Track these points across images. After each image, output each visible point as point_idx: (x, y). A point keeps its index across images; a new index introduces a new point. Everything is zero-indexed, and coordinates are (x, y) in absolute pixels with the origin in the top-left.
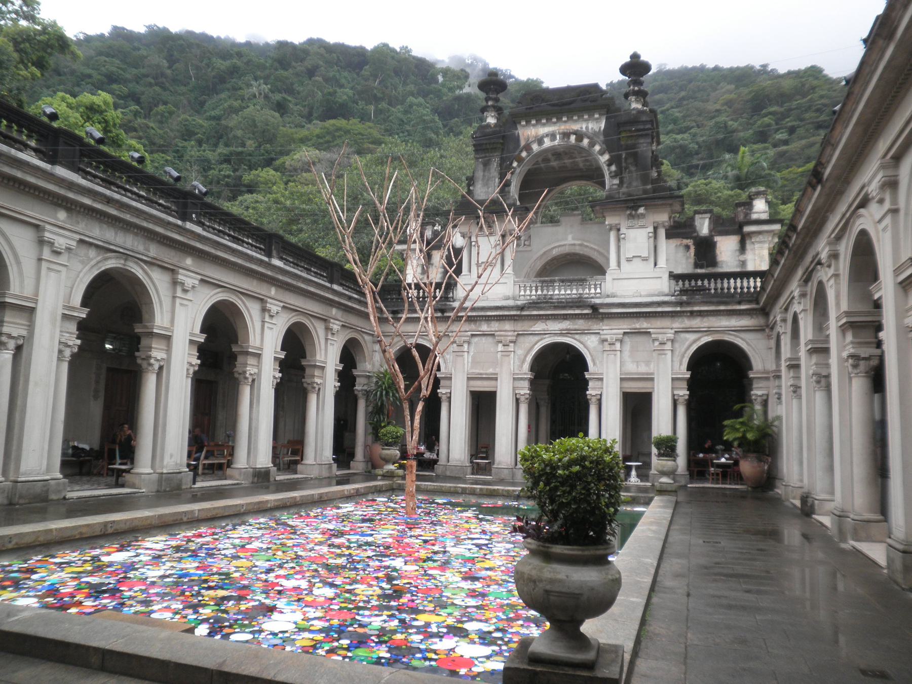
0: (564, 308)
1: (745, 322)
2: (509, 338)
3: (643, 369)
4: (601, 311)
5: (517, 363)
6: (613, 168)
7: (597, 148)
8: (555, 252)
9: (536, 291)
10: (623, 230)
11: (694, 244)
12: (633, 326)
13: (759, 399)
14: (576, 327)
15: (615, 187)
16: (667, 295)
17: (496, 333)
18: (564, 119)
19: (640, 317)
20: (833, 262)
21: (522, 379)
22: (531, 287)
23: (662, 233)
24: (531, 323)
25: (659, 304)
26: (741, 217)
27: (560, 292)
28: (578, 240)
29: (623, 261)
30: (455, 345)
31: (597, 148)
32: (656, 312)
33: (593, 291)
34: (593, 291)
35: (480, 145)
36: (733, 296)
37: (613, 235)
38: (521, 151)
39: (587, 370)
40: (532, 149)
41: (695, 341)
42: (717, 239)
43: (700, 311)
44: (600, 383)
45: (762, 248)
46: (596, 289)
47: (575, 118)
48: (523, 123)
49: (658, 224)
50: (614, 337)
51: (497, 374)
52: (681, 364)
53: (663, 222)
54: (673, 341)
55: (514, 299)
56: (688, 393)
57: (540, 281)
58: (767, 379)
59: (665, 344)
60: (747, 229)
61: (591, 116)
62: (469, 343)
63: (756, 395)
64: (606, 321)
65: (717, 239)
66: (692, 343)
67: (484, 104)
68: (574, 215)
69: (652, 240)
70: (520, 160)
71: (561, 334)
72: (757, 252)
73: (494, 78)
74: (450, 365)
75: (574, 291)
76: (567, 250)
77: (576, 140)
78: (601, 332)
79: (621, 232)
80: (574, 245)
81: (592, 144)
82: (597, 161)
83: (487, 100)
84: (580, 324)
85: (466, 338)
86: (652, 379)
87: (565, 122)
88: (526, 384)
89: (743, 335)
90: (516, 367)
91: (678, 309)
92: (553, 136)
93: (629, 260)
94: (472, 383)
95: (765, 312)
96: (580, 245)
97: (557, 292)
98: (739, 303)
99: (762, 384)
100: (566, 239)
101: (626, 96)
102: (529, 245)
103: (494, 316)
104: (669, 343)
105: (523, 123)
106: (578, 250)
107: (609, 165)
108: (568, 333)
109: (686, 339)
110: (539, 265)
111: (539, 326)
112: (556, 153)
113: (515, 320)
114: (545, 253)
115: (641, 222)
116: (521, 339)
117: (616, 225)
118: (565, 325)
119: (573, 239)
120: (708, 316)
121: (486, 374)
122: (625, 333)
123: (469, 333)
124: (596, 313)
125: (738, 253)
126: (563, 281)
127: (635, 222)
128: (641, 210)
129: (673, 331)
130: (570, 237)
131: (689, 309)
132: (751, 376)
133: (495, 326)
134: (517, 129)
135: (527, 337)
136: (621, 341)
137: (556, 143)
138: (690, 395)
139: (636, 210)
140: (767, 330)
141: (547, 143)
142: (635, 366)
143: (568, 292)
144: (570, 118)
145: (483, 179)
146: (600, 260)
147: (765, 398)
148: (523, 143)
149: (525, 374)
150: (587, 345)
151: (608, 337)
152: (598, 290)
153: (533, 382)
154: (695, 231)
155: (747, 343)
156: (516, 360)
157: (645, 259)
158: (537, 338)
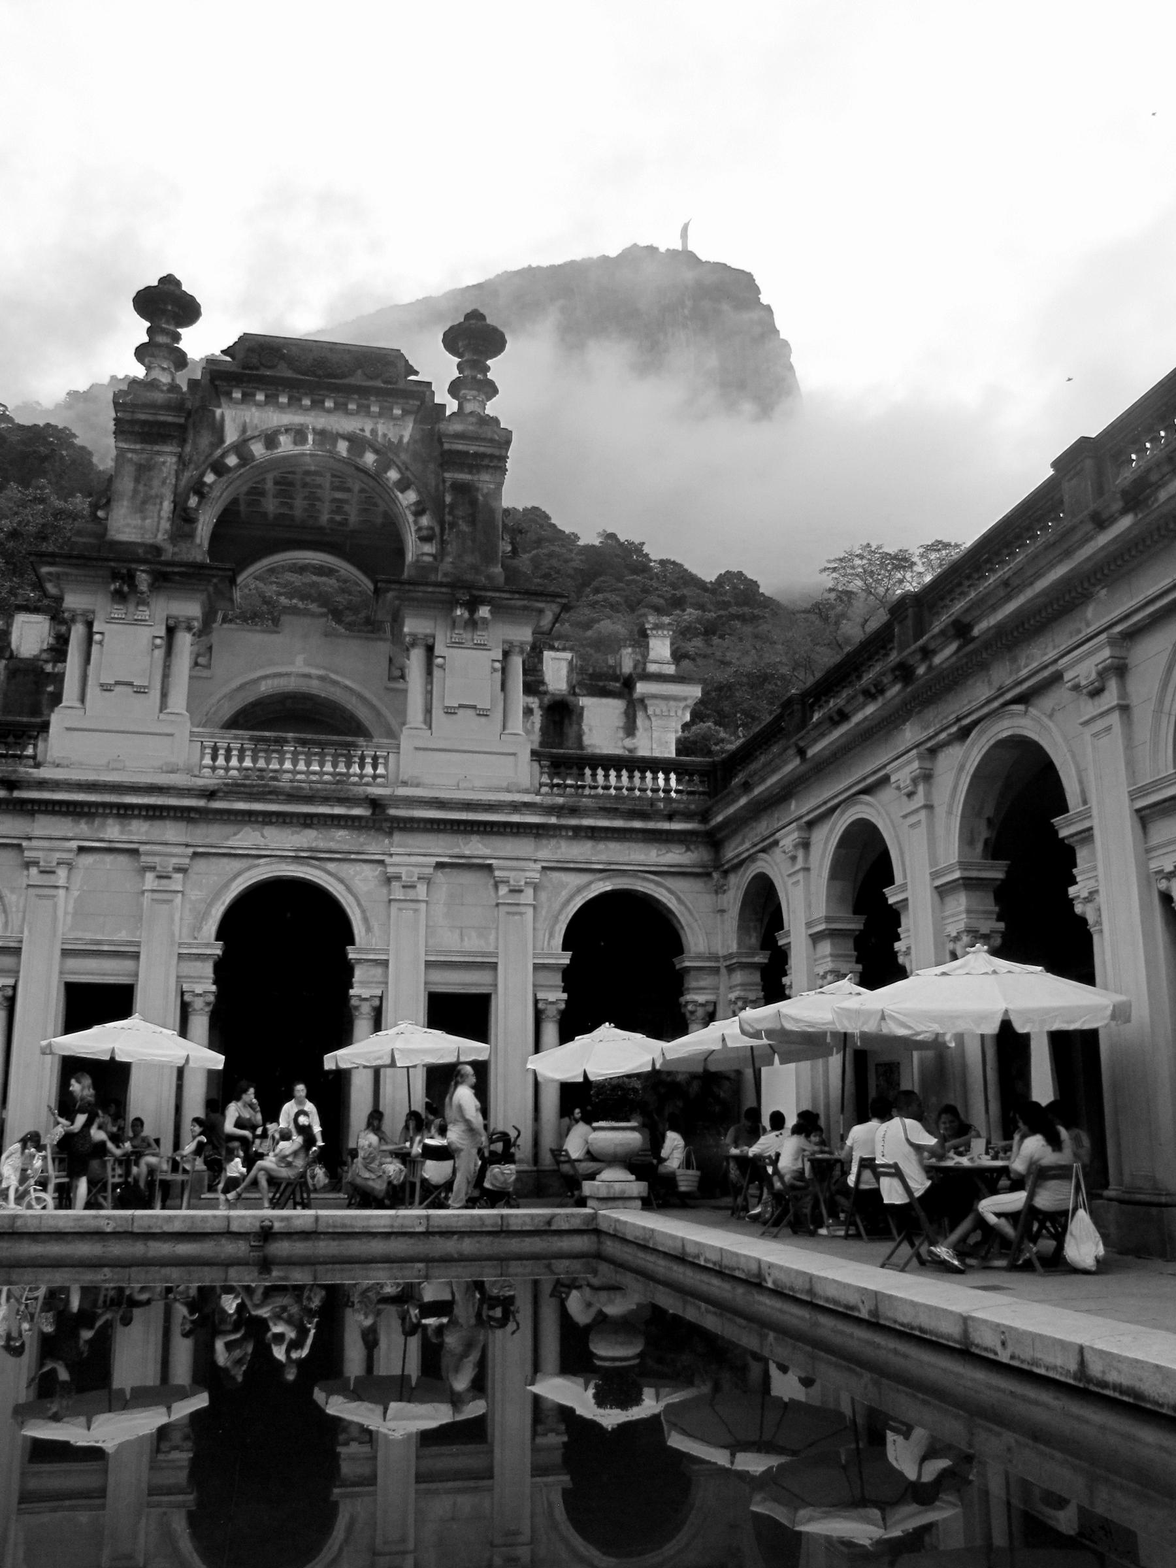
0: (309, 799)
1: (675, 856)
2: (175, 860)
3: (473, 945)
4: (392, 812)
6: (425, 521)
7: (393, 475)
8: (265, 688)
9: (241, 759)
10: (439, 649)
11: (540, 707)
12: (456, 851)
13: (700, 1012)
14: (332, 845)
16: (527, 791)
17: (142, 848)
19: (472, 832)
20: (1113, 685)
21: (199, 957)
22: (228, 750)
23: (517, 662)
24: (229, 829)
25: (516, 807)
26: (627, 667)
27: (295, 766)
28: (317, 667)
29: (437, 712)
30: (34, 871)
31: (393, 475)
32: (506, 825)
33: (369, 770)
34: (369, 770)
35: (133, 422)
36: (652, 802)
37: (416, 658)
38: (223, 456)
39: (352, 943)
41: (579, 890)
42: (584, 701)
43: (593, 829)
44: (379, 971)
45: (665, 729)
46: (375, 767)
48: (237, 395)
49: (511, 643)
50: (416, 870)
51: (138, 944)
52: (551, 935)
53: (522, 643)
54: (536, 887)
55: (189, 771)
56: (565, 996)
57: (251, 739)
58: (716, 971)
59: (521, 891)
60: (641, 688)
63: (695, 1002)
64: (397, 837)
65: (584, 701)
66: (574, 893)
68: (313, 615)
69: (499, 675)
70: (219, 469)
71: (296, 859)
72: (655, 735)
73: (172, 288)
74: (16, 919)
75: (328, 768)
76: (290, 685)
77: (349, 450)
78: (388, 860)
79: (437, 652)
80: (308, 676)
81: (385, 465)
82: (394, 500)
84: (341, 838)
85: (65, 856)
86: (494, 966)
87: (329, 411)
88: (208, 969)
89: (669, 882)
90: (185, 931)
91: (553, 820)
92: (299, 435)
93: (450, 712)
94: (72, 963)
95: (714, 840)
96: (322, 678)
97: (288, 765)
98: (670, 818)
99: (706, 981)
100: (292, 663)
102: (208, 666)
104: (529, 892)
106: (315, 687)
107: (418, 514)
108: (313, 857)
109: (563, 886)
110: (228, 711)
111: (247, 838)
112: (288, 478)
113: (190, 820)
114: (241, 687)
115: (480, 637)
116: (201, 865)
117: (426, 636)
119: (307, 663)
120: (607, 839)
121: (111, 943)
122: (440, 866)
123: (74, 844)
124: (379, 817)
125: (621, 734)
126: (303, 743)
127: (467, 635)
128: (484, 612)
129: (538, 866)
130: (299, 660)
131: (573, 822)
132: (687, 964)
133: (139, 830)
135: (214, 860)
136: (428, 881)
138: (567, 1002)
139: (472, 610)
140: (715, 875)
141: (286, 445)
142: (456, 936)
143: (315, 767)
145: (133, 497)
146: (363, 713)
147: (710, 1008)
149: (207, 945)
150: (352, 886)
151: (403, 871)
152: (381, 770)
153: (221, 968)
154: (543, 683)
155: (679, 899)
157: (483, 714)
158: (237, 865)
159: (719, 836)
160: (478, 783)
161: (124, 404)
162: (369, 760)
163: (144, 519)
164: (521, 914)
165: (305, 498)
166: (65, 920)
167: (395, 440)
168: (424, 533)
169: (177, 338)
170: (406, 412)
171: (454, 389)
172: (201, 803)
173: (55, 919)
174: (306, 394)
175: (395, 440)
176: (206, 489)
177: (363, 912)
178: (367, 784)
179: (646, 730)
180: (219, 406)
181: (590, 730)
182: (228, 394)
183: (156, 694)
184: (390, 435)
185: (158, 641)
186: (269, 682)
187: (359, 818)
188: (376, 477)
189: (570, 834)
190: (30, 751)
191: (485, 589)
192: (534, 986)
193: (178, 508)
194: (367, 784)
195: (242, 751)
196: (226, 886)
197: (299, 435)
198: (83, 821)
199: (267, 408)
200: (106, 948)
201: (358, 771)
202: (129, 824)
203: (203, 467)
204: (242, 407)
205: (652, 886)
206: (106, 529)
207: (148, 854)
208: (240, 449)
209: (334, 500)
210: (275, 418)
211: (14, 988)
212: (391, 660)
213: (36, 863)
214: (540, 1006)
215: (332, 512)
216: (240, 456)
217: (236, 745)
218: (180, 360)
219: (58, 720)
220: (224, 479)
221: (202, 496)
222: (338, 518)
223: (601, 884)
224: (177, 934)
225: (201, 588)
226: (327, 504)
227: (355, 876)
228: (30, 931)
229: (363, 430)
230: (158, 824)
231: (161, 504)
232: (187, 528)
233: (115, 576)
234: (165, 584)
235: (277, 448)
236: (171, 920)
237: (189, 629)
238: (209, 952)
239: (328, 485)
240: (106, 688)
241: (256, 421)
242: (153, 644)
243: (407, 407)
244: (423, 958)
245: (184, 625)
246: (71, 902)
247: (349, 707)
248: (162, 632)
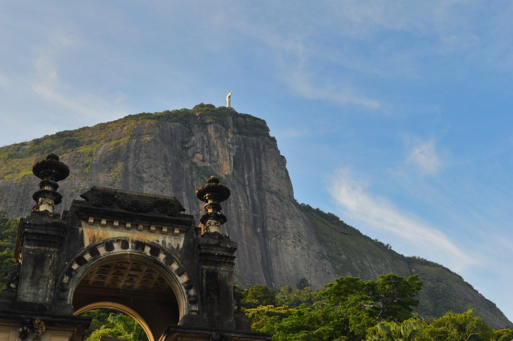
6: (192, 292)
7: (175, 266)
15: (194, 313)
18: (141, 227)
31: (175, 266)
40: (99, 253)
47: (153, 228)
48: (91, 220)
61: (171, 232)
67: (37, 189)
70: (81, 261)
81: (170, 260)
83: (42, 185)
87: (140, 230)
92: (125, 244)
101: (204, 219)
105: (91, 220)
134: (81, 226)
137: (129, 251)
141: (117, 249)
144: (147, 228)
145: (32, 277)
148: (87, 243)
161: (29, 224)
163: (38, 290)
167: (175, 247)
168: (192, 299)
169: (56, 187)
170: (181, 232)
171: (204, 219)
174: (129, 221)
175: (175, 247)
176: (73, 273)
180: (81, 226)
182: (86, 220)
184: (172, 244)
188: (165, 268)
191: (229, 332)
197: (125, 244)
199: (106, 228)
203: (72, 260)
204: (94, 227)
206: (16, 295)
208: (93, 250)
209: (129, 275)
210: (112, 234)
215: (127, 281)
216: (92, 254)
218: (58, 199)
220: (83, 267)
221: (71, 276)
222: (128, 284)
225: (71, 329)
226: (125, 278)
229: (158, 241)
231: (48, 281)
232: (62, 295)
233: (23, 323)
234: (50, 328)
235: (112, 250)
239: (129, 267)
241: (101, 235)
243: (182, 229)
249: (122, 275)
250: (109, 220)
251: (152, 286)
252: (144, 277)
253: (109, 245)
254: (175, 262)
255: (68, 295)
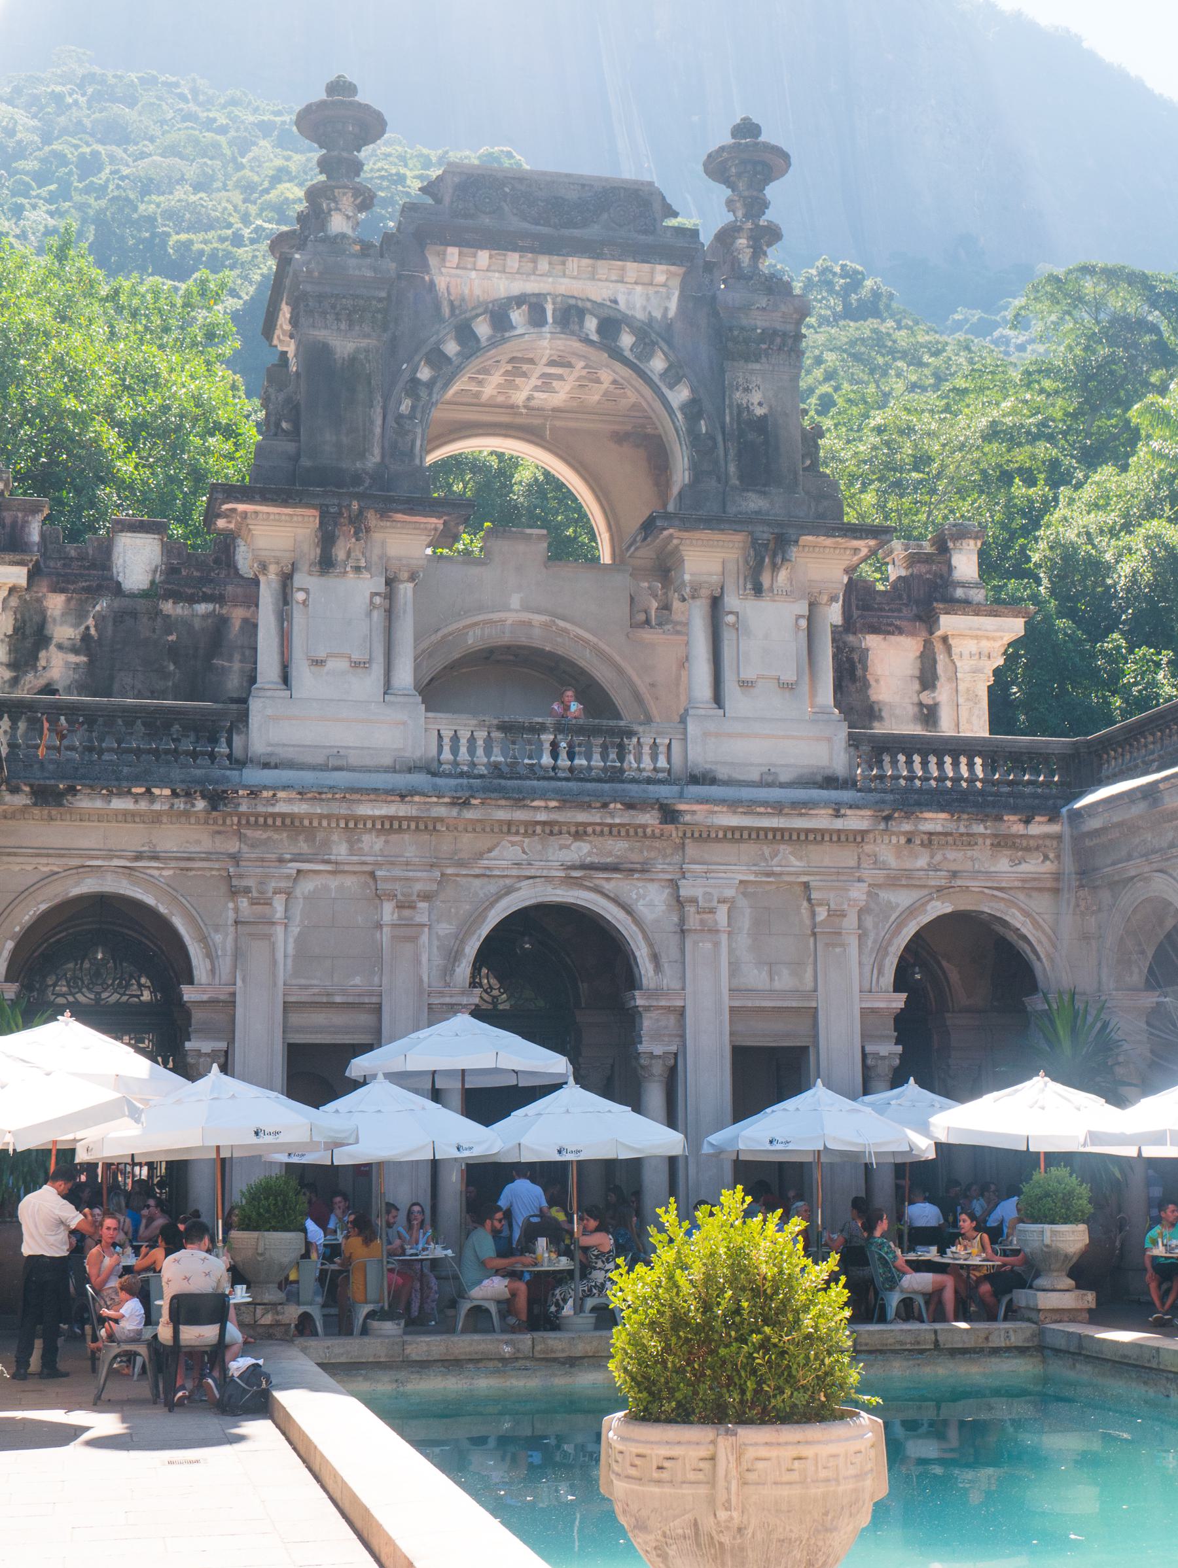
2: (418, 887)
3: (784, 980)
4: (688, 818)
5: (438, 961)
8: (473, 640)
9: (488, 751)
10: (732, 601)
17: (378, 873)
22: (472, 740)
28: (538, 611)
30: (244, 903)
31: (658, 364)
33: (647, 763)
34: (647, 763)
41: (911, 911)
42: (872, 641)
46: (654, 757)
55: (432, 769)
60: (948, 623)
62: (289, 894)
69: (803, 635)
70: (437, 358)
71: (570, 882)
74: (225, 965)
77: (600, 330)
80: (529, 624)
93: (746, 685)
94: (295, 1019)
96: (545, 625)
103: (374, 819)
106: (537, 639)
111: (507, 854)
118: (581, 851)
119: (526, 608)
125: (916, 686)
129: (864, 886)
130: (515, 601)
138: (902, 1057)
142: (764, 975)
151: (698, 892)
156: (435, 950)
159: (1088, 843)
160: (784, 777)
162: (646, 750)
164: (842, 945)
165: (507, 373)
166: (285, 965)
167: (657, 314)
172: (454, 812)
173: (274, 962)
175: (659, 317)
176: (423, 393)
177: (650, 945)
178: (649, 781)
179: (949, 680)
181: (877, 681)
182: (442, 256)
183: (378, 669)
185: (378, 600)
186: (478, 632)
187: (644, 827)
189: (903, 840)
190: (223, 749)
192: (865, 1036)
193: (390, 417)
194: (649, 781)
195: (489, 741)
196: (482, 916)
198: (301, 838)
200: (338, 999)
201: (635, 765)
202: (359, 840)
205: (1002, 906)
207: (386, 879)
209: (543, 375)
211: (226, 1052)
212: (632, 598)
213: (247, 890)
214: (869, 1062)
215: (536, 388)
217: (481, 735)
219: (255, 705)
223: (938, 904)
224: (425, 979)
226: (534, 381)
227: (640, 897)
228: (244, 981)
229: (615, 302)
230: (394, 837)
236: (417, 961)
237: (412, 578)
238: (465, 1001)
240: (318, 663)
242: (371, 602)
244: (726, 1003)
245: (405, 575)
246: (291, 940)
247: (582, 663)
248: (381, 588)
249: (524, 375)
250: (494, 252)
251: (597, 398)
252: (579, 378)
253: (499, 318)
254: (660, 354)
255: (413, 442)
